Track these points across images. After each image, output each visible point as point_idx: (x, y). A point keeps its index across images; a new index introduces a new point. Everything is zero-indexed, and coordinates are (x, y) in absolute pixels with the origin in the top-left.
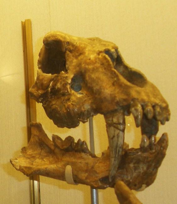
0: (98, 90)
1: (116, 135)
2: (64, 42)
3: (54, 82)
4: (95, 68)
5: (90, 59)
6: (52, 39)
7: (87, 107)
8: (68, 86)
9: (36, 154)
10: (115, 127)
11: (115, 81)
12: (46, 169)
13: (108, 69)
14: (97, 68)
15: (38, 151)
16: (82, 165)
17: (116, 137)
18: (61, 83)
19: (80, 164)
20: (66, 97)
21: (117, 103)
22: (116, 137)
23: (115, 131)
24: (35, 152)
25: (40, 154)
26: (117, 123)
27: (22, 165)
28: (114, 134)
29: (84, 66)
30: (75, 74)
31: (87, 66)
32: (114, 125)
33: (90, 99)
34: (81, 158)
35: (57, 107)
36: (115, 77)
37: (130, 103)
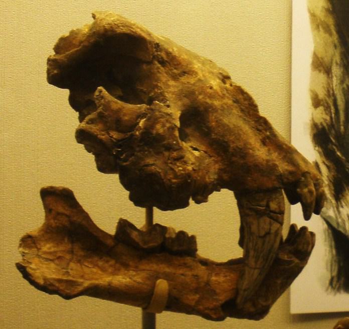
0: (241, 149)
1: (272, 231)
2: (150, 42)
3: (149, 119)
4: (225, 107)
5: (211, 88)
6: (125, 30)
7: (212, 177)
8: (177, 133)
9: (64, 251)
10: (271, 218)
11: (268, 137)
12: (109, 285)
13: (249, 112)
14: (229, 107)
15: (65, 246)
16: (188, 279)
17: (272, 236)
18: (164, 126)
19: (183, 277)
20: (175, 154)
21: (280, 177)
22: (272, 236)
23: (271, 224)
24: (61, 248)
25: (71, 252)
26: (277, 211)
27: (49, 276)
28: (270, 229)
29: (203, 98)
30: (182, 111)
31: (208, 101)
32: (272, 214)
33: (216, 162)
34: (185, 265)
35: (160, 171)
36: (266, 130)
37: (301, 179)
